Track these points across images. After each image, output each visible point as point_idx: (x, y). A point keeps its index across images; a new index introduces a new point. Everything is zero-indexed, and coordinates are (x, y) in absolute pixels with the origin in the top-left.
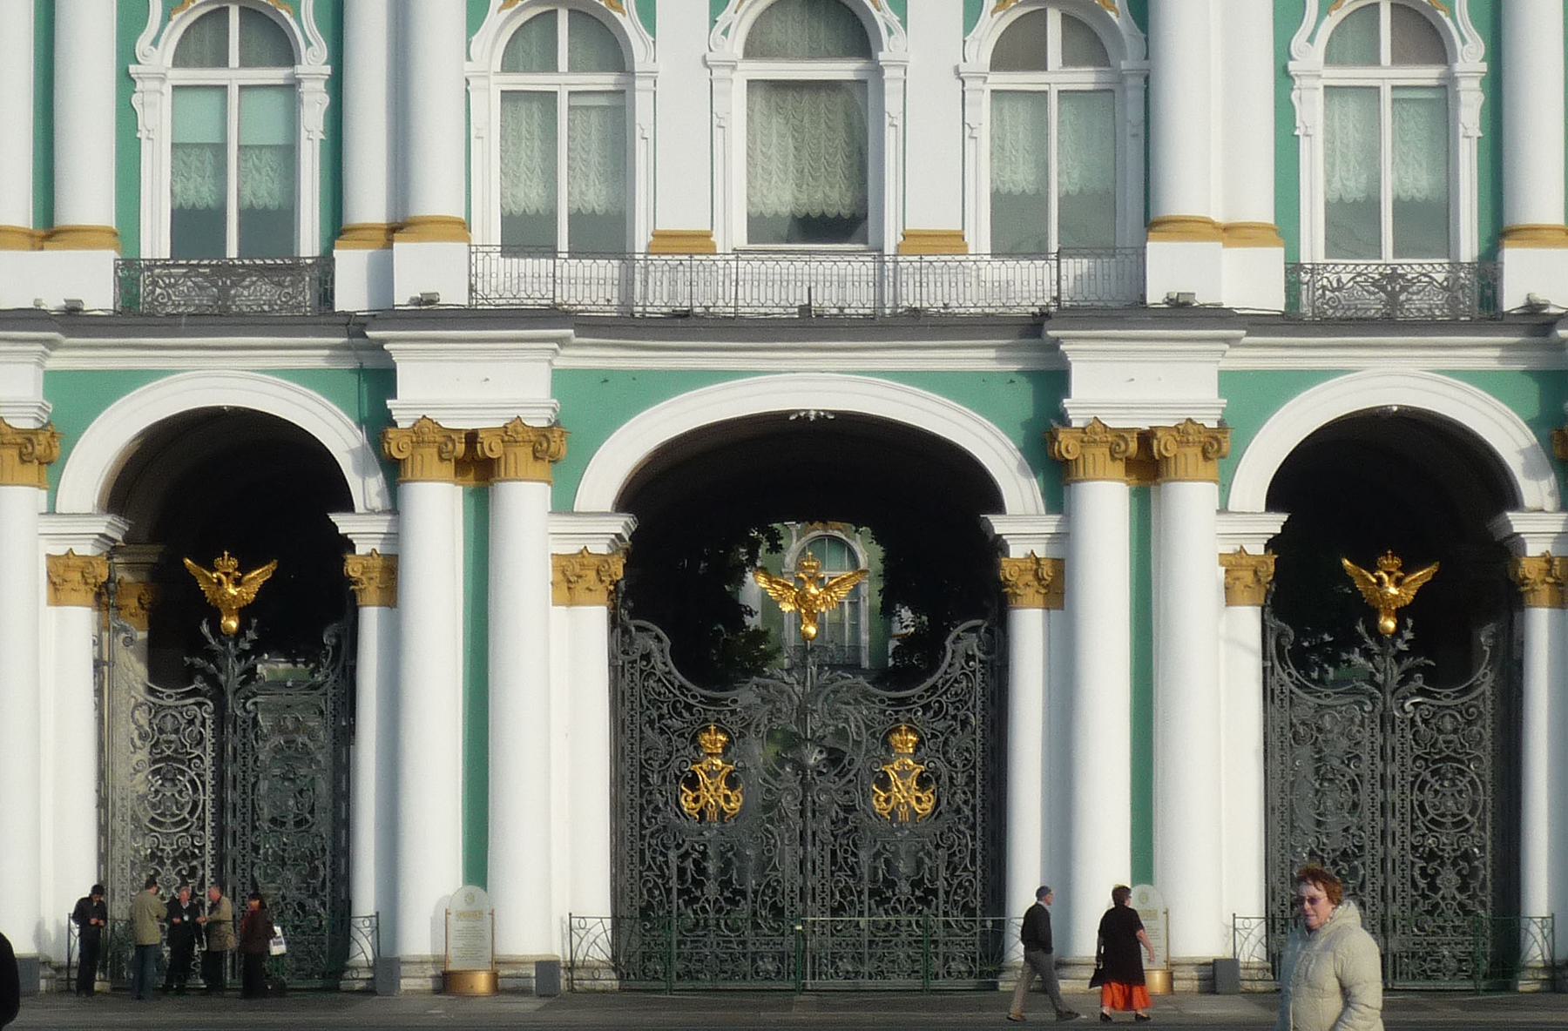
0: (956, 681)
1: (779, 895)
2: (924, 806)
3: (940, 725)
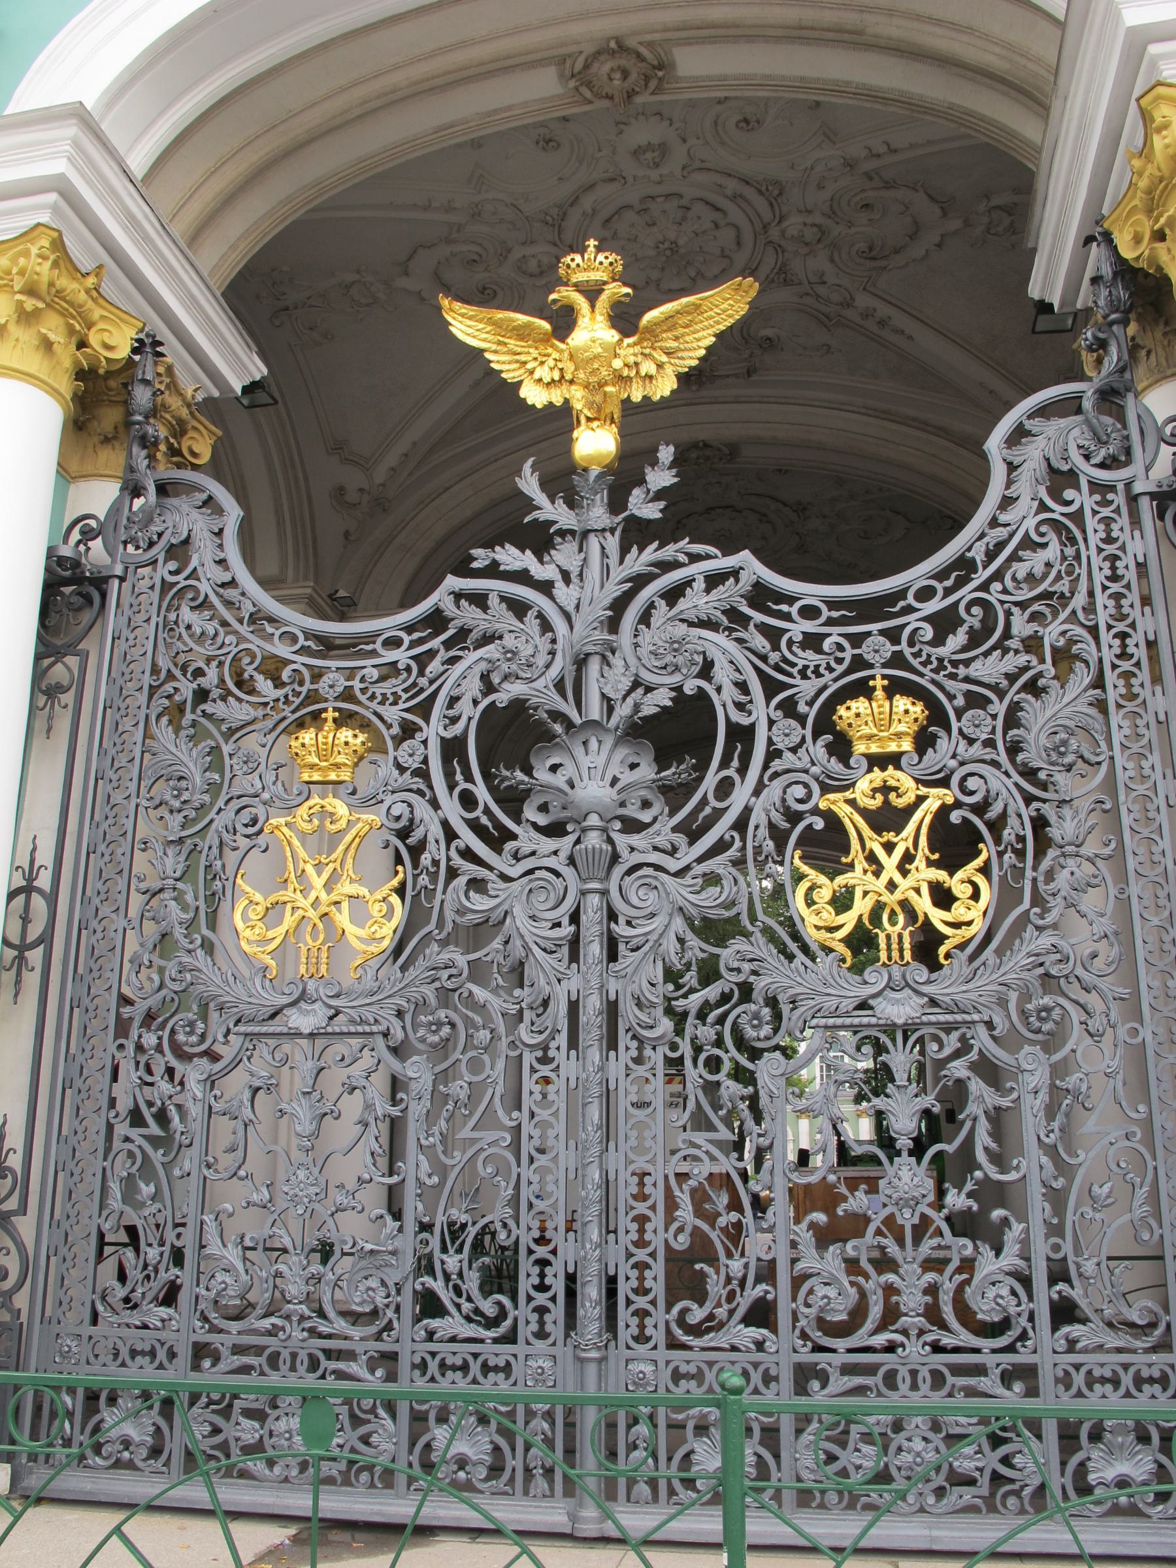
0: (1028, 543)
2: (959, 911)
3: (990, 668)
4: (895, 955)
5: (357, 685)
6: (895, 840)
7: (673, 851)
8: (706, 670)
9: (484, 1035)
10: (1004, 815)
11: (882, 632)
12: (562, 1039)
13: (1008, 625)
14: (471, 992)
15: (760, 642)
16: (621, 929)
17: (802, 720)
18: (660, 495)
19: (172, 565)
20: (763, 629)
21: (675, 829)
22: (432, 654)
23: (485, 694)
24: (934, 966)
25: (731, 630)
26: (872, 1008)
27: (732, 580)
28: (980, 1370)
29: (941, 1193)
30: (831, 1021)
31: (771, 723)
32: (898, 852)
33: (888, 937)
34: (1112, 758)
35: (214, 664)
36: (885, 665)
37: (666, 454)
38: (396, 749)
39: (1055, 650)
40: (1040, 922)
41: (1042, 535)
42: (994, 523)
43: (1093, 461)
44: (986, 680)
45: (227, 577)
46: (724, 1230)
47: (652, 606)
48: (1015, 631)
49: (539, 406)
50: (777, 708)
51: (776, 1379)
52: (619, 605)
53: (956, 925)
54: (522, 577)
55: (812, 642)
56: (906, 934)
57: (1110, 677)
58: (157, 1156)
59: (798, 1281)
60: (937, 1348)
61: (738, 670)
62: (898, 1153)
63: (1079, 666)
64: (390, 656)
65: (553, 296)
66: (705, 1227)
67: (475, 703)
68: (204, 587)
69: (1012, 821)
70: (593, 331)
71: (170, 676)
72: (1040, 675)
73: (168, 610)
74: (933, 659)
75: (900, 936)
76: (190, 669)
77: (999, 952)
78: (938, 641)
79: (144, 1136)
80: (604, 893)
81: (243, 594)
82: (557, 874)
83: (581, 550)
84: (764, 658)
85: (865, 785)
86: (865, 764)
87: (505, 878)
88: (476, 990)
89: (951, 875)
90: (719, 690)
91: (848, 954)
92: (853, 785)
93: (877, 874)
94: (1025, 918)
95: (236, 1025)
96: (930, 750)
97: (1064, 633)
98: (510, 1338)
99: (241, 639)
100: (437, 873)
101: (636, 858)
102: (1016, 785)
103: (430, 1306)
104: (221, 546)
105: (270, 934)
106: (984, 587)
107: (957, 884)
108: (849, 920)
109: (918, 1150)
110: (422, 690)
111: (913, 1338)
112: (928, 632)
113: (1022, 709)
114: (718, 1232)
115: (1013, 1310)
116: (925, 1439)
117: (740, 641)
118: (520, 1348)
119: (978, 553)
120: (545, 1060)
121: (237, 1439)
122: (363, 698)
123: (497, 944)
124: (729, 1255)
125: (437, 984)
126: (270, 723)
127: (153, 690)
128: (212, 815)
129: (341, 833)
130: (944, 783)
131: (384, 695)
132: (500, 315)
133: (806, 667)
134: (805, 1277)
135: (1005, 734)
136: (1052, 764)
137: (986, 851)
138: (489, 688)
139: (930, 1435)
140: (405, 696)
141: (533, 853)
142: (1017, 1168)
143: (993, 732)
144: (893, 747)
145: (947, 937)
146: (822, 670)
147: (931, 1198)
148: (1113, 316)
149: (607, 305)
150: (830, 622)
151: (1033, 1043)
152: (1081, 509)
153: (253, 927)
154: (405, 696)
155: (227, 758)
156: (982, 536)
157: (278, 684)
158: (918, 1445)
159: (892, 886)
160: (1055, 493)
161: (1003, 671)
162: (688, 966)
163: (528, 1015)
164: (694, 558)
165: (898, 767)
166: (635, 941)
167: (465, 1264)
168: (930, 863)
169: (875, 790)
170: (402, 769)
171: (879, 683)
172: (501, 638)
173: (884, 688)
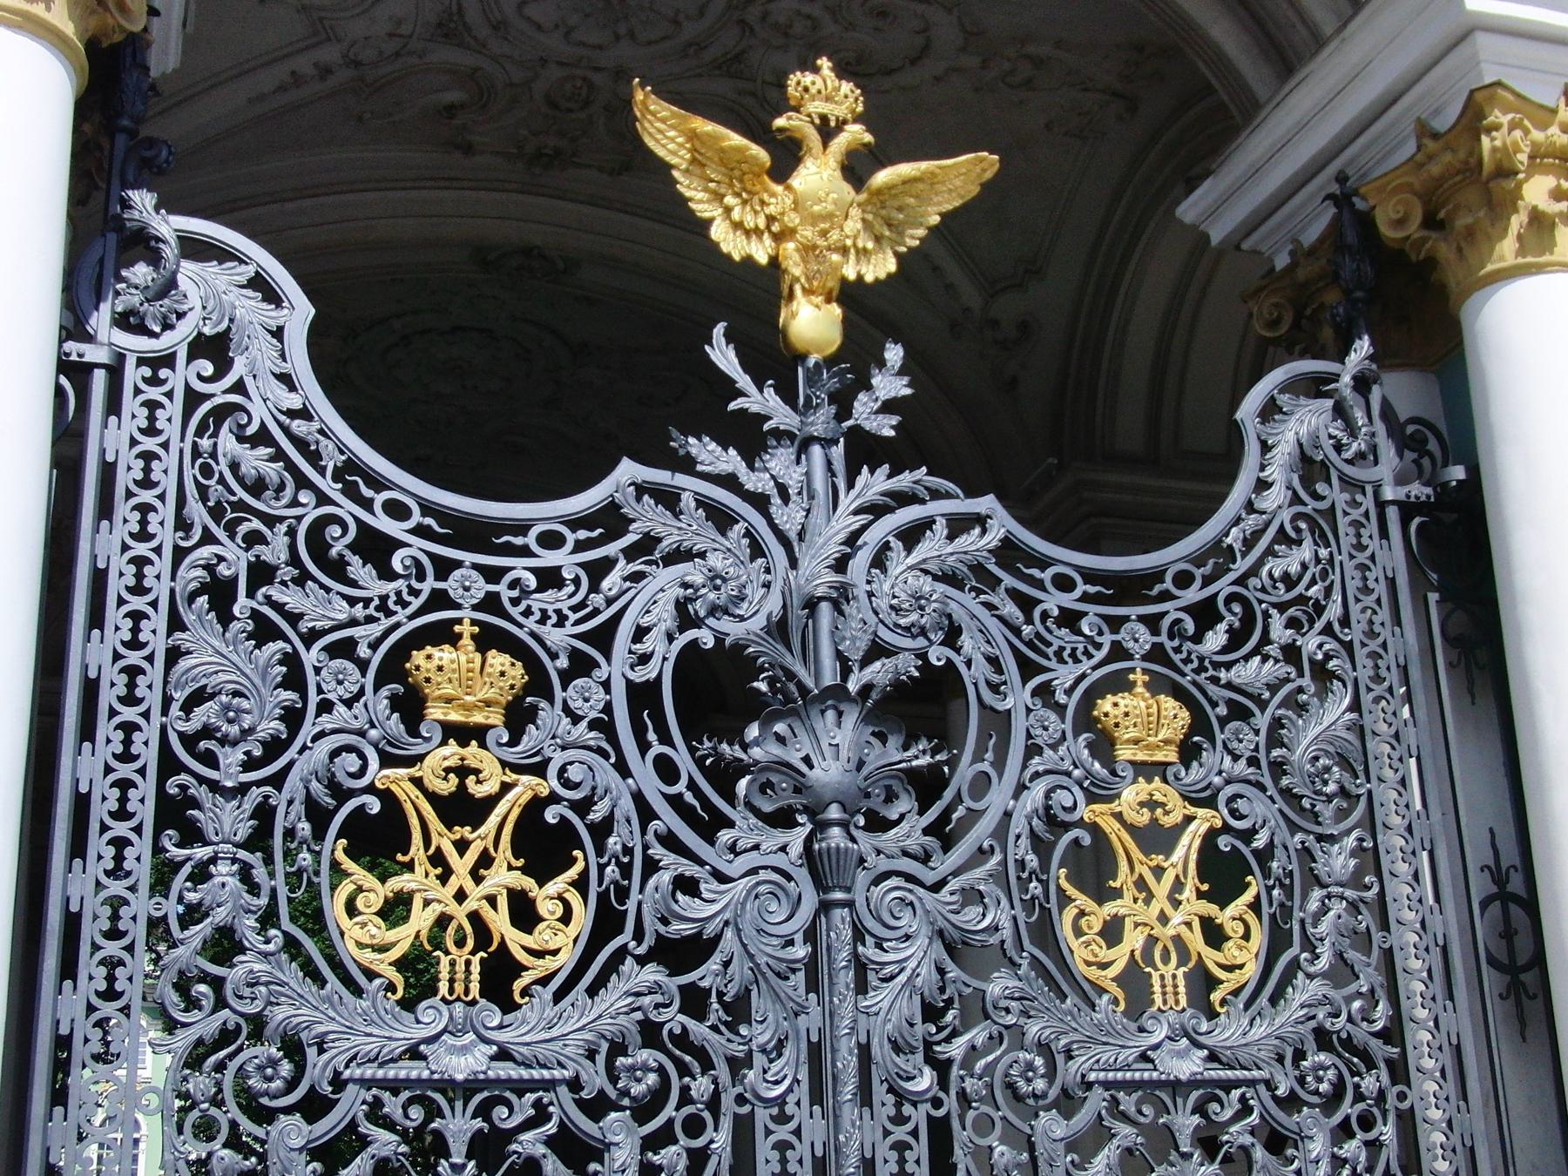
3: (1251, 672)
5: (506, 594)
6: (1166, 865)
7: (925, 858)
8: (952, 636)
9: (701, 1086)
11: (1142, 619)
12: (803, 1091)
14: (684, 1028)
15: (1010, 609)
16: (868, 951)
17: (1060, 709)
18: (888, 407)
19: (208, 368)
20: (1014, 594)
21: (926, 832)
22: (607, 565)
23: (682, 629)
25: (979, 592)
26: (424, 1058)
27: (977, 531)
31: (1029, 710)
32: (1168, 878)
33: (1162, 977)
34: (1370, 792)
35: (283, 528)
37: (894, 354)
38: (564, 689)
39: (1312, 661)
40: (1312, 969)
41: (1298, 530)
42: (1250, 507)
44: (1250, 690)
45: (294, 401)
47: (886, 547)
48: (1274, 635)
49: (737, 257)
50: (1034, 693)
52: (852, 539)
53: (1230, 969)
54: (729, 482)
55: (1069, 619)
61: (988, 642)
64: (549, 558)
67: (670, 638)
68: (259, 412)
71: (208, 538)
72: (1300, 690)
73: (200, 432)
74: (1193, 656)
76: (243, 529)
78: (1198, 638)
80: (850, 904)
82: (789, 878)
83: (798, 462)
84: (1017, 631)
85: (1131, 794)
86: (1129, 773)
87: (722, 878)
88: (691, 1024)
90: (969, 664)
91: (1121, 996)
92: (1118, 796)
94: (1295, 965)
95: (347, 1066)
96: (1195, 764)
97: (1320, 646)
99: (323, 499)
100: (631, 863)
101: (884, 864)
102: (1280, 811)
104: (283, 357)
105: (391, 935)
106: (1241, 581)
108: (1119, 956)
110: (596, 612)
113: (1283, 727)
117: (989, 606)
119: (1234, 538)
120: (782, 1119)
122: (515, 612)
123: (714, 964)
125: (638, 1015)
126: (375, 630)
127: (180, 554)
128: (291, 753)
129: (491, 801)
130: (1210, 802)
131: (544, 612)
133: (1062, 649)
135: (1268, 752)
136: (1316, 793)
138: (686, 619)
140: (573, 617)
141: (756, 847)
143: (1256, 749)
145: (1222, 982)
146: (1080, 656)
148: (1359, 294)
150: (1085, 598)
151: (1311, 1106)
153: (364, 925)
154: (573, 617)
155: (310, 672)
156: (1237, 521)
157: (387, 574)
160: (1307, 482)
162: (949, 1003)
163: (759, 1060)
164: (936, 495)
168: (1200, 895)
170: (576, 719)
171: (1138, 677)
172: (702, 555)
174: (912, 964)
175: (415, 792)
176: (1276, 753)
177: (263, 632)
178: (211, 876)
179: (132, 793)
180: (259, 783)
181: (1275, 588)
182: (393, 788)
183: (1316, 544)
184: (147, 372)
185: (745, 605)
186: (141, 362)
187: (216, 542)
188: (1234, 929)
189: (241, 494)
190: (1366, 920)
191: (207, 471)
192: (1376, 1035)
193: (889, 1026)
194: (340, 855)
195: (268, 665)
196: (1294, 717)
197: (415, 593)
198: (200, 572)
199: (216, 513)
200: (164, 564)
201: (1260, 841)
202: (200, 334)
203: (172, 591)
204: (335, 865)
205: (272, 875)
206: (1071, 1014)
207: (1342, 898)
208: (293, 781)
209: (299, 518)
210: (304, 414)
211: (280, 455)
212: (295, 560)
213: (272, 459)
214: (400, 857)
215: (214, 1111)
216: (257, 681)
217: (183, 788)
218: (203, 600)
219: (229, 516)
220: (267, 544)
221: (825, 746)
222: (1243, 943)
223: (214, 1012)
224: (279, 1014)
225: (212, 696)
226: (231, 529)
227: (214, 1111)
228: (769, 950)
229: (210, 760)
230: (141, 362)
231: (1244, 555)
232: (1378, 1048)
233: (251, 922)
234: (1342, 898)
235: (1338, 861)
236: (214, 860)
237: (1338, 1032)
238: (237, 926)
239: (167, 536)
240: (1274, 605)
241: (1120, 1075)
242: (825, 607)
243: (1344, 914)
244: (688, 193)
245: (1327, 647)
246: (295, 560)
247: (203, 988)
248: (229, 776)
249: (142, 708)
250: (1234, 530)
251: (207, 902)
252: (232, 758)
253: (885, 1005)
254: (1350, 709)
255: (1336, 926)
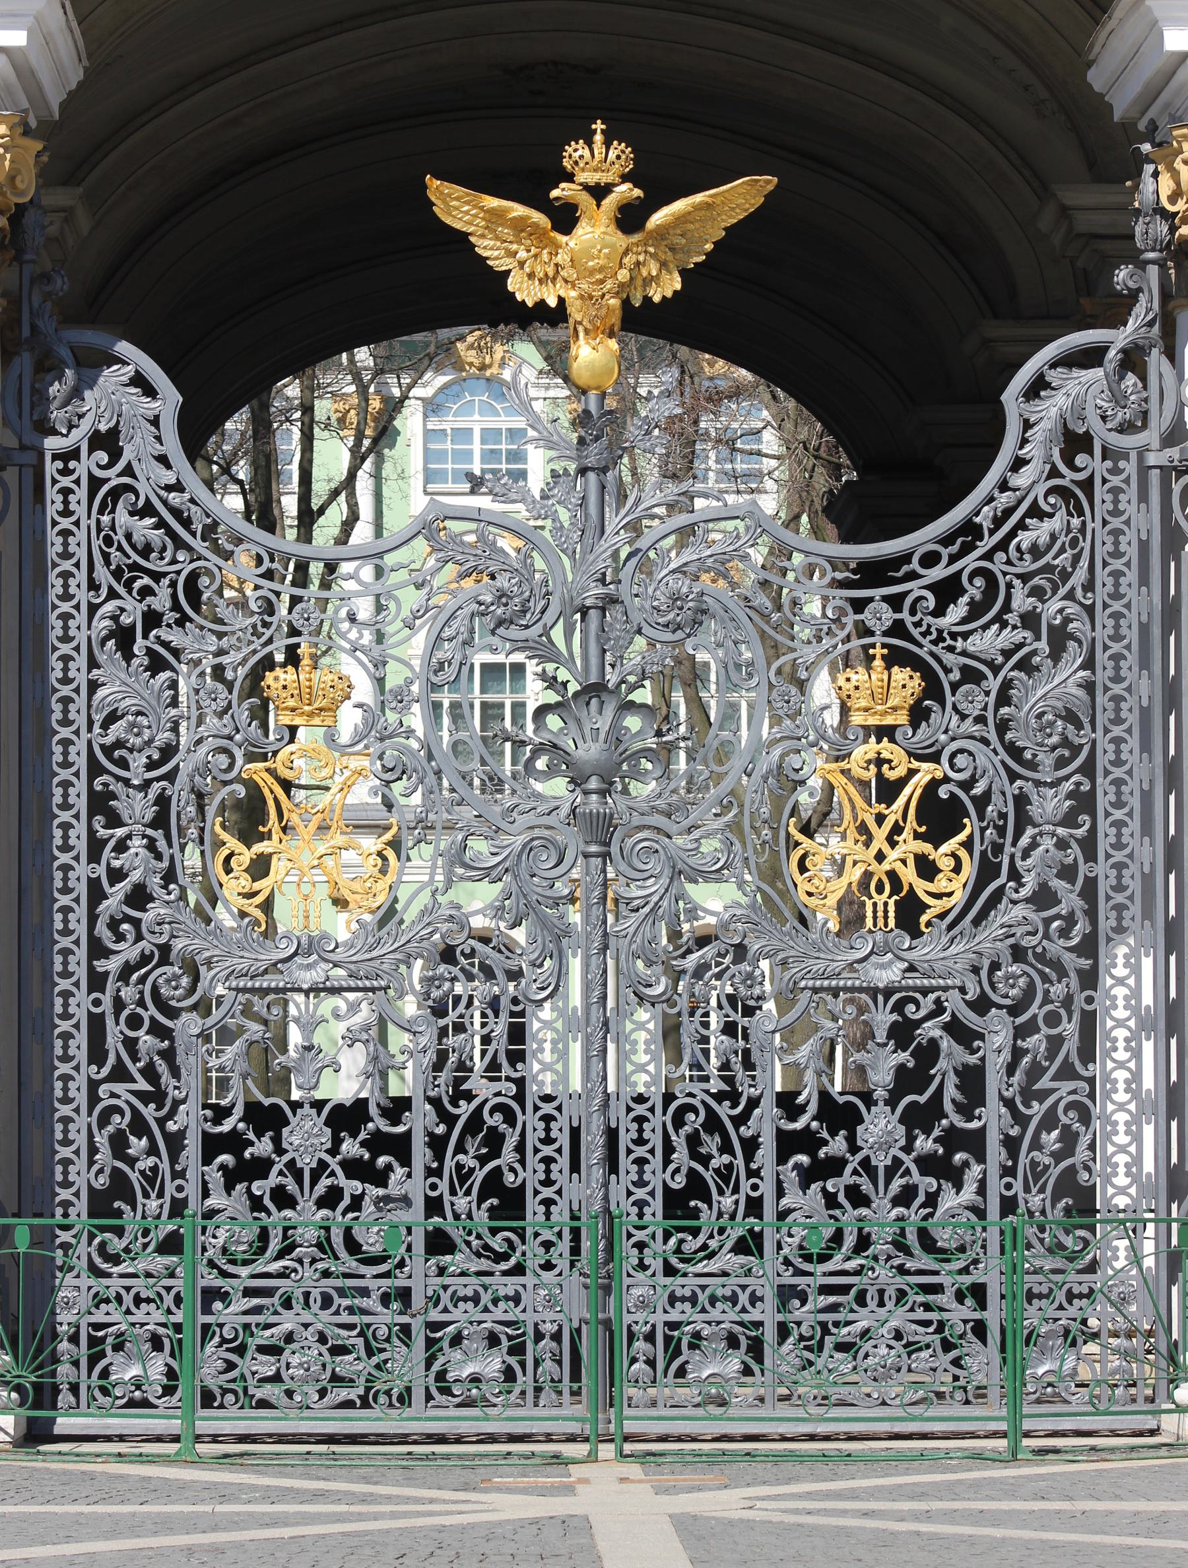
0: (1035, 512)
1: (508, 1155)
2: (941, 884)
3: (988, 642)
4: (881, 923)
10: (987, 794)
11: (885, 599)
13: (1008, 597)
19: (103, 457)
24: (916, 933)
28: (937, 1289)
29: (911, 1139)
30: (818, 983)
31: (771, 686)
33: (875, 904)
34: (1094, 742)
36: (886, 634)
40: (1015, 896)
42: (1004, 486)
43: (1109, 426)
44: (983, 656)
45: (170, 478)
46: (717, 1171)
48: (1015, 605)
49: (530, 304)
51: (761, 1299)
56: (891, 902)
57: (1101, 657)
58: (149, 1112)
59: (782, 1215)
60: (902, 1270)
62: (876, 1103)
63: (1071, 645)
65: (555, 193)
66: (700, 1168)
68: (143, 488)
69: (996, 797)
70: (595, 232)
71: (113, 595)
72: (1034, 653)
73: (101, 512)
74: (933, 629)
75: (886, 904)
76: (138, 584)
77: (976, 922)
78: (939, 612)
79: (133, 1092)
81: (192, 501)
84: (766, 617)
89: (936, 849)
93: (867, 844)
94: (999, 893)
96: (924, 724)
97: (1061, 611)
98: (519, 1270)
102: (1003, 762)
103: (439, 1243)
104: (159, 439)
105: (257, 886)
106: (988, 556)
107: (941, 855)
109: (892, 1102)
111: (882, 1263)
112: (931, 603)
114: (711, 1172)
115: (968, 1238)
116: (890, 1347)
118: (529, 1280)
121: (254, 1373)
124: (721, 1192)
130: (935, 758)
132: (493, 202)
134: (790, 1211)
135: (996, 710)
137: (970, 826)
139: (893, 1343)
142: (980, 1118)
143: (985, 709)
144: (889, 720)
147: (903, 1142)
149: (614, 207)
151: (1000, 1007)
152: (1092, 476)
156: (991, 499)
158: (883, 1350)
159: (880, 857)
161: (999, 647)
165: (892, 740)
166: (636, 902)
167: (474, 1205)
168: (917, 836)
169: (869, 762)
173: (883, 657)
174: (655, 898)
175: (270, 780)
176: (1004, 710)
177: (156, 664)
178: (128, 848)
179: (71, 790)
180: (158, 779)
181: (1021, 559)
182: (255, 777)
183: (1070, 514)
184: (59, 465)
185: (528, 616)
186: (55, 457)
187: (119, 597)
188: (946, 864)
189: (135, 557)
190: (1075, 852)
191: (108, 541)
192: (1068, 949)
193: (634, 946)
194: (218, 829)
195: (161, 691)
196: (1025, 678)
197: (266, 625)
198: (107, 622)
199: (117, 574)
200: (82, 618)
201: (978, 790)
202: (97, 432)
203: (89, 638)
204: (214, 834)
205: (170, 846)
206: (789, 934)
207: (1053, 834)
208: (182, 778)
209: (178, 573)
210: (178, 487)
211: (161, 524)
212: (176, 607)
213: (156, 527)
214: (261, 828)
215: (139, 1010)
216: (154, 703)
217: (106, 785)
218: (111, 644)
219: (127, 575)
220: (155, 595)
221: (587, 731)
222: (953, 875)
223: (135, 942)
224: (178, 945)
225: (123, 716)
226: (128, 585)
227: (139, 1010)
228: (539, 890)
229: (123, 764)
230: (55, 457)
231: (992, 532)
232: (1072, 962)
233: (157, 880)
234: (1053, 834)
235: (1049, 804)
236: (129, 837)
237: (1034, 947)
238: (148, 883)
239: (83, 596)
240: (1018, 576)
241: (826, 983)
242: (593, 613)
243: (1052, 849)
244: (485, 254)
245: (1069, 611)
246: (176, 607)
247: (125, 926)
248: (137, 777)
249: (74, 728)
250: (986, 509)
251: (126, 867)
252: (138, 762)
253: (631, 930)
254: (1083, 667)
255: (1042, 859)
